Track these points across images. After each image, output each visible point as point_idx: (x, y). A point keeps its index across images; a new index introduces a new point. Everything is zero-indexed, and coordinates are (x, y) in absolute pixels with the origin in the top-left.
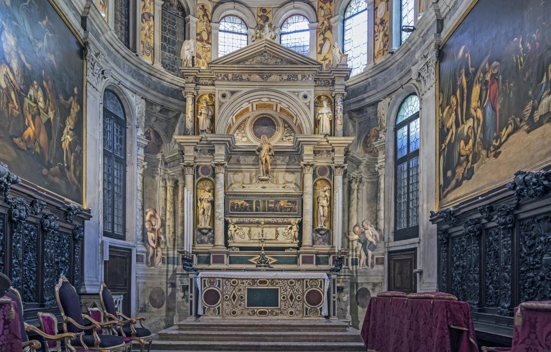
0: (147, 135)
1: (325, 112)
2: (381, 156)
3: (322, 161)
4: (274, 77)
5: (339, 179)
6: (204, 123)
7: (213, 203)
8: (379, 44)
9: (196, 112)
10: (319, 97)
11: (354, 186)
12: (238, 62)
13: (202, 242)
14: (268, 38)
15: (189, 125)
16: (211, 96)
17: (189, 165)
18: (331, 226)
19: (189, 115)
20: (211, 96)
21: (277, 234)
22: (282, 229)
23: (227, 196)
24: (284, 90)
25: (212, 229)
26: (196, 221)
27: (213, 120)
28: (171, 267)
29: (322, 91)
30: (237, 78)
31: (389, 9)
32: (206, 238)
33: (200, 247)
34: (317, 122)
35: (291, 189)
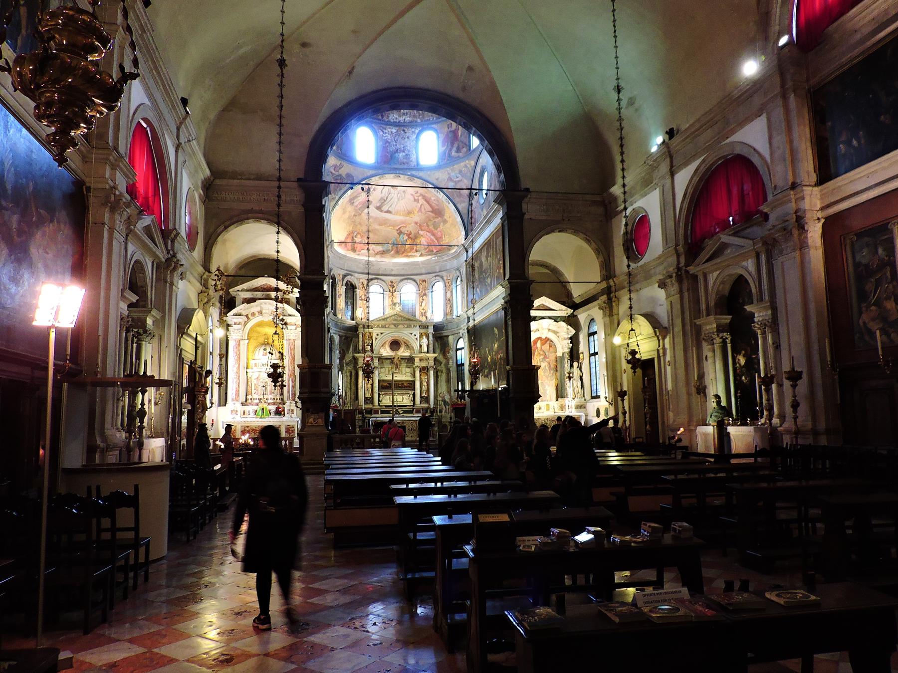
0: (340, 353)
1: (425, 341)
2: (451, 361)
3: (424, 364)
5: (432, 373)
8: (448, 310)
11: (439, 374)
15: (361, 348)
18: (429, 395)
19: (361, 343)
22: (405, 397)
25: (372, 398)
29: (423, 331)
31: (452, 295)
33: (367, 406)
34: (421, 346)
35: (410, 379)
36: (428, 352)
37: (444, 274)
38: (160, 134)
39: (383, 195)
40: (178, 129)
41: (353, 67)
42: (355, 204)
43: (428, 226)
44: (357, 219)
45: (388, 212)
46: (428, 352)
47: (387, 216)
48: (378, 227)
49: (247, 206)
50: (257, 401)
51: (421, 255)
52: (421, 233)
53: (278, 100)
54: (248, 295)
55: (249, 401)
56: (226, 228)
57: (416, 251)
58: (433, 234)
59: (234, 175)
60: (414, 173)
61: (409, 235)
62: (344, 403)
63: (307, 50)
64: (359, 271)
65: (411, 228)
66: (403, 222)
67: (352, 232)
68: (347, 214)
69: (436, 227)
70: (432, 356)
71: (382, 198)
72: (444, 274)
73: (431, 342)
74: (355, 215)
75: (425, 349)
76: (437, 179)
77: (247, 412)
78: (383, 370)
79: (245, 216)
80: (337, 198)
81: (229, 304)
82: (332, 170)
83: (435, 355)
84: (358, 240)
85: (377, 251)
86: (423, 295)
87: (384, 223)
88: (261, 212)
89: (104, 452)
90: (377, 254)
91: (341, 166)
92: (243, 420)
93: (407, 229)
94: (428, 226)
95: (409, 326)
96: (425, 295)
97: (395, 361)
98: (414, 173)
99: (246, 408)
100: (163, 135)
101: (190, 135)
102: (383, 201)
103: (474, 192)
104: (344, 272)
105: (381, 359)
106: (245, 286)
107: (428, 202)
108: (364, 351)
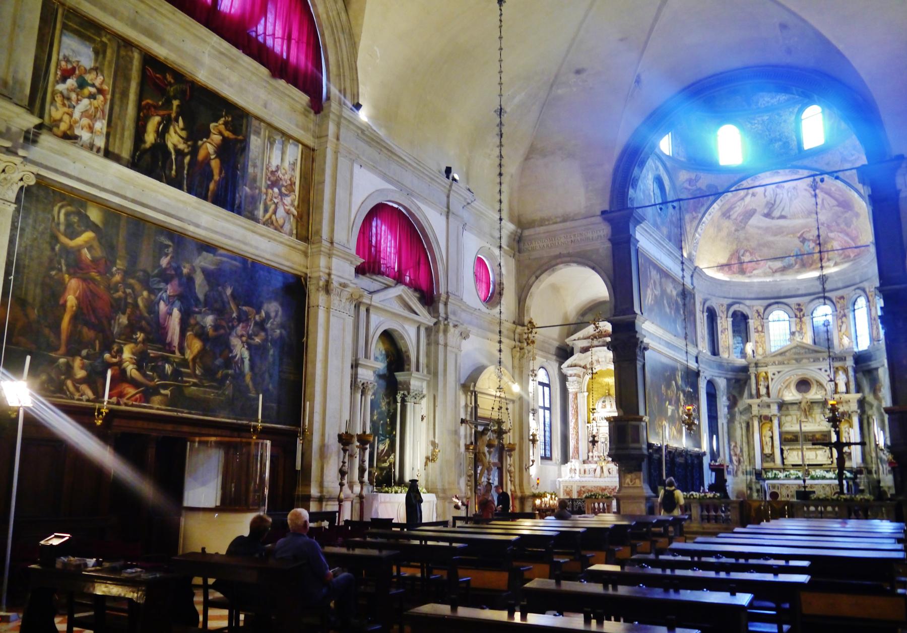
0: (729, 399)
1: (841, 379)
4: (804, 361)
6: (763, 391)
7: (772, 438)
9: (757, 384)
10: (837, 368)
12: (782, 354)
13: (767, 462)
14: (799, 339)
15: (754, 392)
16: (766, 373)
17: (756, 416)
19: (754, 386)
20: (766, 373)
21: (817, 455)
22: (820, 452)
23: (781, 434)
24: (811, 368)
25: (773, 454)
26: (762, 449)
27: (768, 388)
28: (749, 477)
29: (837, 364)
30: (781, 363)
32: (769, 459)
33: (766, 465)
36: (847, 392)
38: (413, 210)
39: (768, 198)
40: (448, 197)
41: (639, 76)
42: (734, 217)
43: (838, 225)
44: (742, 234)
45: (782, 217)
46: (847, 392)
47: (782, 222)
48: (771, 239)
49: (555, 252)
50: (596, 459)
51: (836, 264)
52: (831, 235)
53: (498, 150)
54: (585, 343)
55: (590, 459)
56: (537, 278)
57: (829, 260)
58: (847, 235)
59: (542, 222)
62: (739, 461)
63: (584, 76)
64: (753, 296)
67: (737, 251)
68: (724, 233)
69: (848, 225)
70: (854, 397)
71: (768, 203)
73: (852, 379)
74: (736, 230)
75: (842, 388)
76: (828, 164)
77: (587, 471)
78: (789, 418)
79: (553, 262)
80: (700, 215)
81: (564, 353)
82: (686, 185)
83: (859, 395)
84: (747, 258)
86: (841, 316)
87: (779, 232)
88: (569, 255)
89: (321, 500)
90: (776, 272)
91: (697, 179)
92: (583, 479)
94: (838, 225)
95: (816, 360)
96: (845, 315)
97: (803, 405)
99: (586, 466)
100: (419, 208)
101: (465, 199)
103: (818, 178)
104: (730, 301)
105: (782, 405)
106: (580, 334)
108: (758, 395)
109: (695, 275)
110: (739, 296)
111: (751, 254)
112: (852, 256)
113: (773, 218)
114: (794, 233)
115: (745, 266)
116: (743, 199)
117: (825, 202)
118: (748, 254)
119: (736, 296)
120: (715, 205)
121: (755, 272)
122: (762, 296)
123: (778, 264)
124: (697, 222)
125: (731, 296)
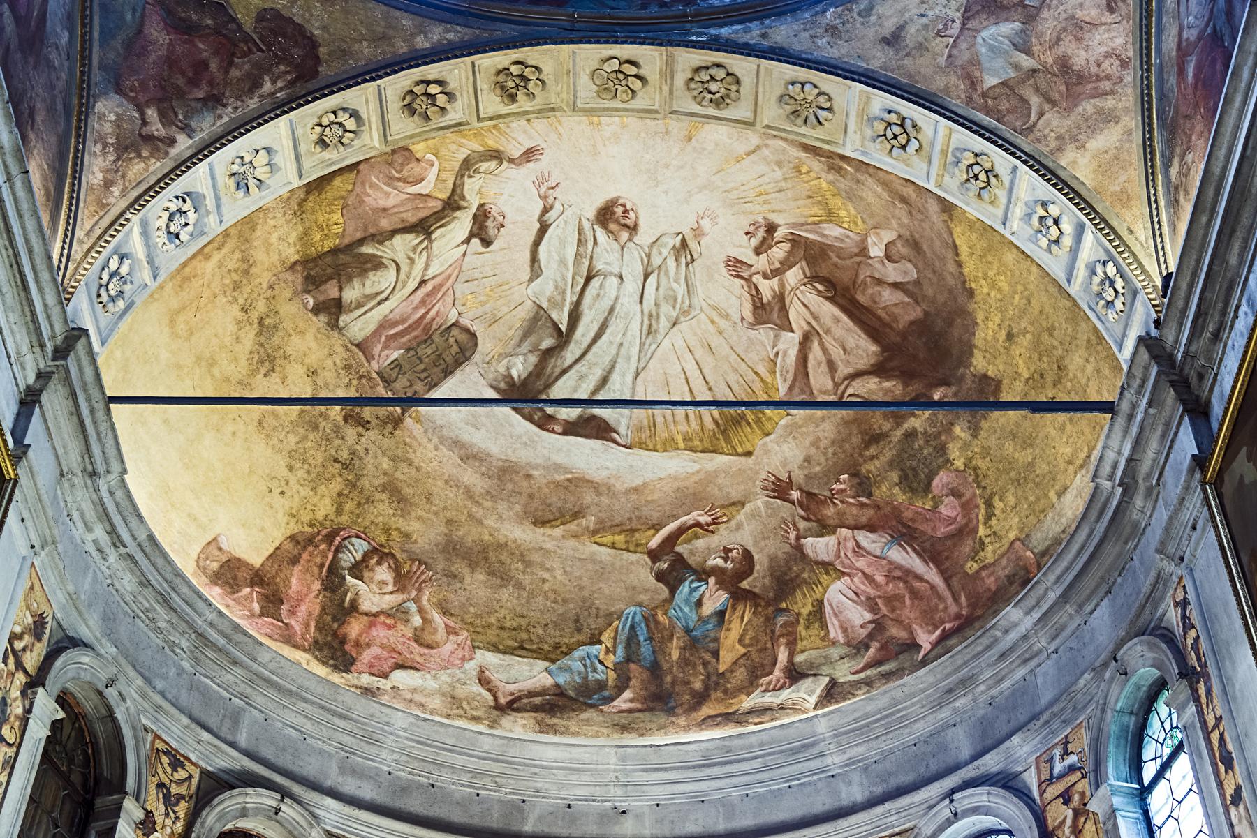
37: (1021, 752)
39: (544, 289)
42: (359, 325)
43: (863, 486)
47: (583, 455)
48: (519, 533)
51: (833, 692)
52: (819, 547)
57: (795, 675)
58: (905, 533)
60: (724, 32)
61: (733, 580)
65: (753, 530)
66: (691, 497)
67: (333, 536)
69: (916, 479)
71: (539, 318)
72: (1021, 752)
76: (893, 40)
80: (184, 144)
85: (507, 689)
87: (559, 506)
90: (512, 706)
93: (723, 537)
98: (724, 32)
102: (554, 335)
104: (228, 760)
107: (843, 294)
109: (53, 401)
110: (286, 761)
111: (402, 581)
112: (926, 639)
113: (545, 423)
114: (626, 530)
115: (354, 628)
116: (423, 228)
117: (816, 352)
118: (383, 573)
119: (267, 752)
120: (276, 132)
121: (399, 677)
122: (414, 805)
123: (531, 674)
124: (157, 167)
125: (243, 739)
